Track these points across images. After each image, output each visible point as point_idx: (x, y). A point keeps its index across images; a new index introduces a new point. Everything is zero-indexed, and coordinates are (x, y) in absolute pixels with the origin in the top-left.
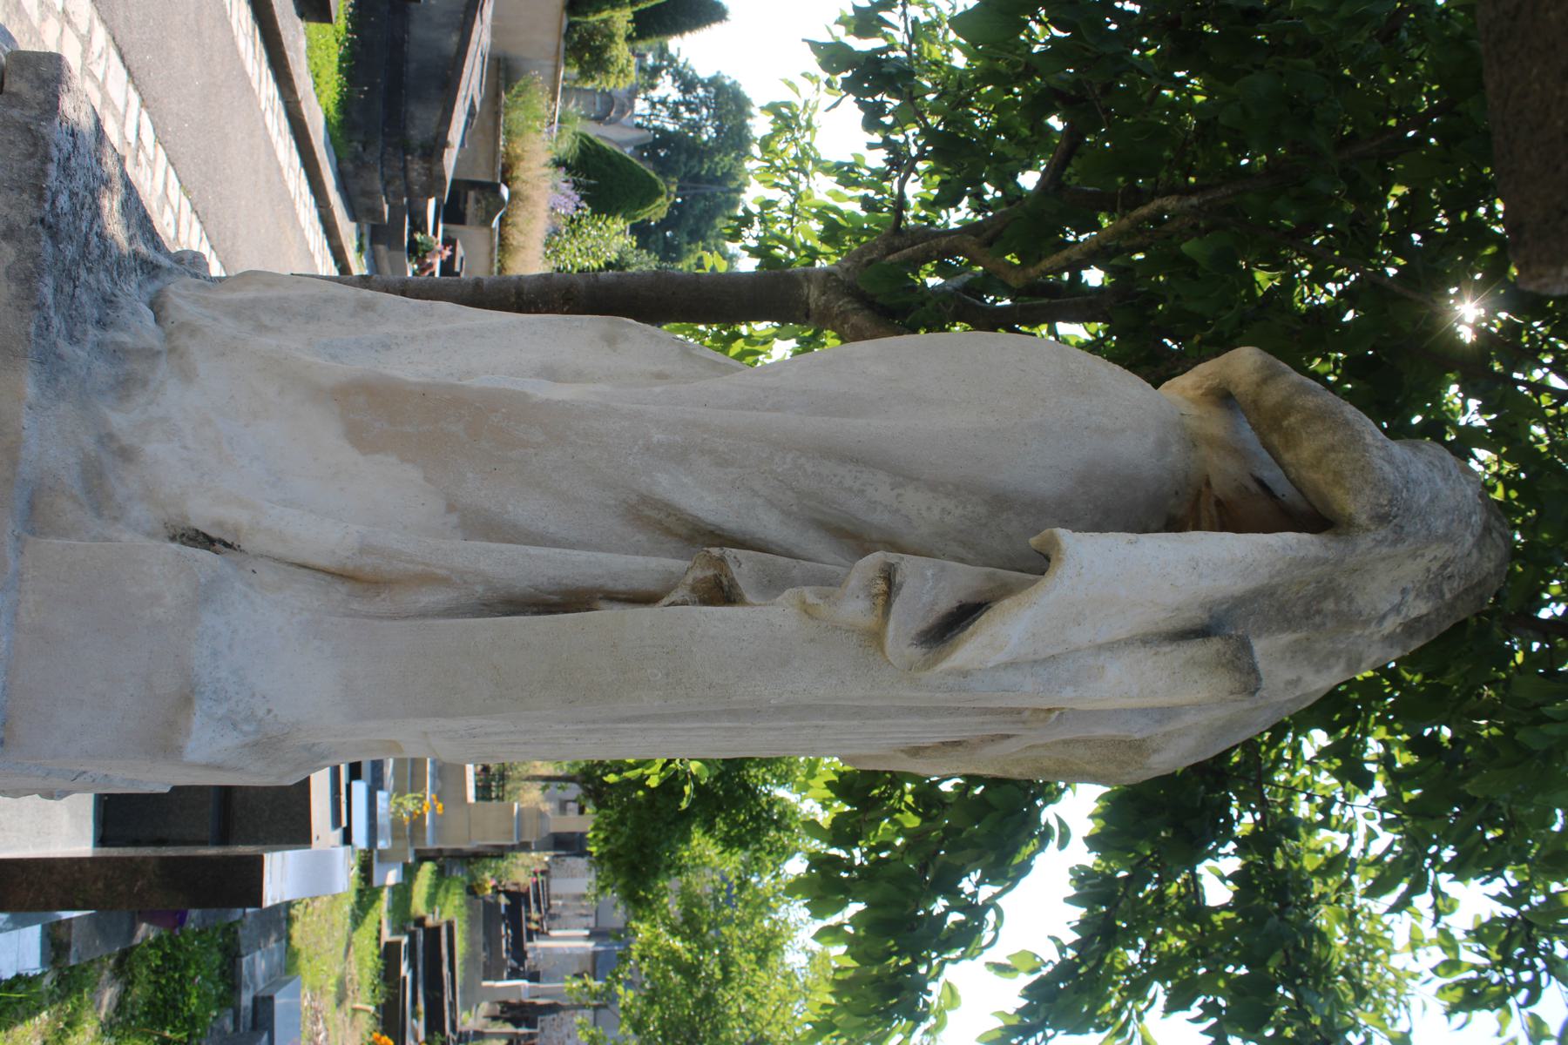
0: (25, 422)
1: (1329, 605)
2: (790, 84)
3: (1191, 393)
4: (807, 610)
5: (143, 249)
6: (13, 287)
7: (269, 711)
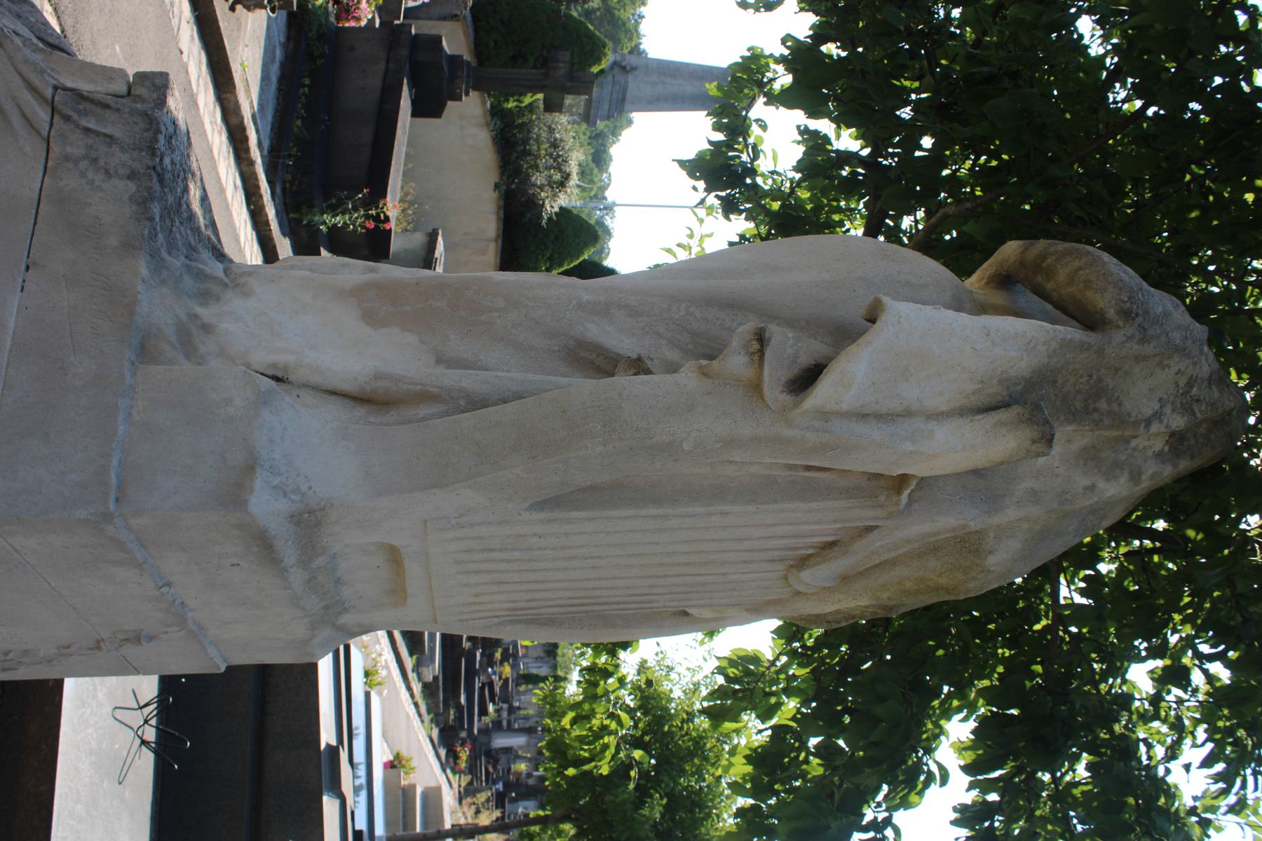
0: (140, 288)
1: (1103, 405)
2: (669, 251)
3: (977, 285)
4: (705, 373)
5: (213, 237)
6: (134, 207)
7: (310, 488)
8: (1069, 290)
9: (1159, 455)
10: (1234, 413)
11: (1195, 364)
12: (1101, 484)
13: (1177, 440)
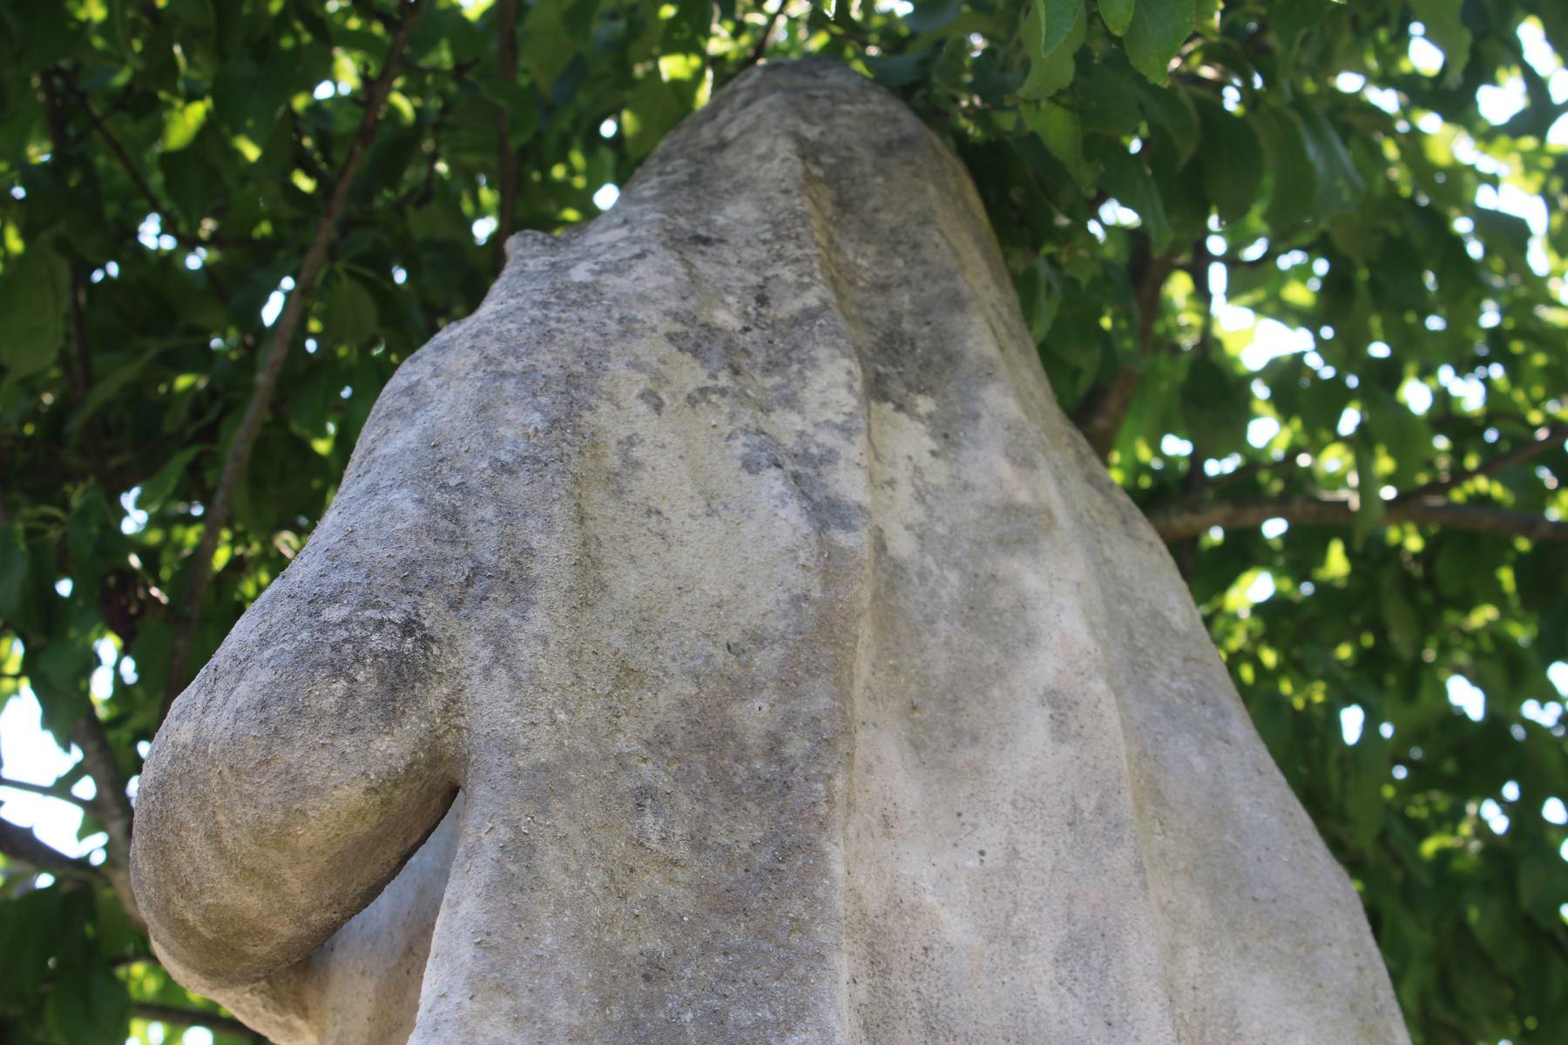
1: (755, 716)
8: (295, 885)
9: (948, 435)
10: (811, 133)
11: (628, 327)
12: (1045, 667)
13: (899, 364)
